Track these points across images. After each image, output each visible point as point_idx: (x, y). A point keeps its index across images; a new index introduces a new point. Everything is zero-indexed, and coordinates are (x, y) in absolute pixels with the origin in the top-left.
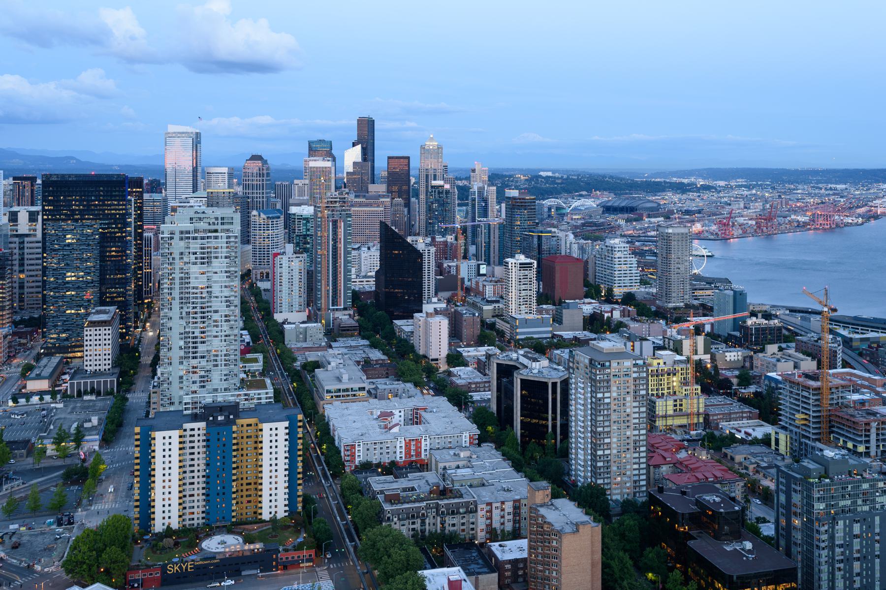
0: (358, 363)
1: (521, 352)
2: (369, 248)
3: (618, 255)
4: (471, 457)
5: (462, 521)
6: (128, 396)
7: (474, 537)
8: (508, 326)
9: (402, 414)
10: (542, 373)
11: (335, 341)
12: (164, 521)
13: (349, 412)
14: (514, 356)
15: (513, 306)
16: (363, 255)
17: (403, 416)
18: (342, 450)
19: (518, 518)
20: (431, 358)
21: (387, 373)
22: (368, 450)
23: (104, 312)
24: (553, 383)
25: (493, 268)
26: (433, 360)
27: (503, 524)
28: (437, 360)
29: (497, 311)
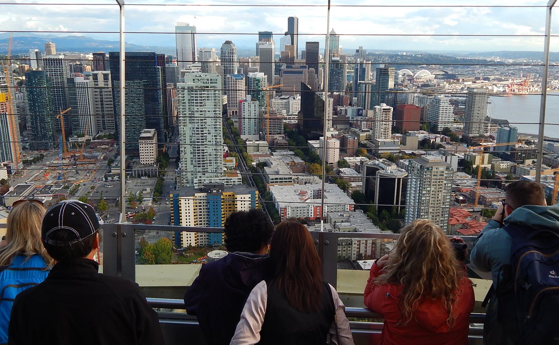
0: (288, 164)
1: (381, 160)
2: (294, 98)
3: (442, 104)
4: (350, 217)
5: (344, 249)
6: (164, 178)
7: (350, 257)
8: (374, 145)
9: (313, 192)
10: (392, 172)
11: (275, 151)
12: (187, 242)
13: (283, 190)
14: (377, 162)
15: (377, 134)
16: (291, 103)
17: (312, 194)
18: (279, 210)
19: (374, 249)
20: (329, 162)
21: (304, 170)
22: (293, 211)
23: (149, 132)
24: (398, 178)
25: (367, 111)
26: (330, 164)
27: (366, 251)
28: (332, 164)
29: (368, 137)
